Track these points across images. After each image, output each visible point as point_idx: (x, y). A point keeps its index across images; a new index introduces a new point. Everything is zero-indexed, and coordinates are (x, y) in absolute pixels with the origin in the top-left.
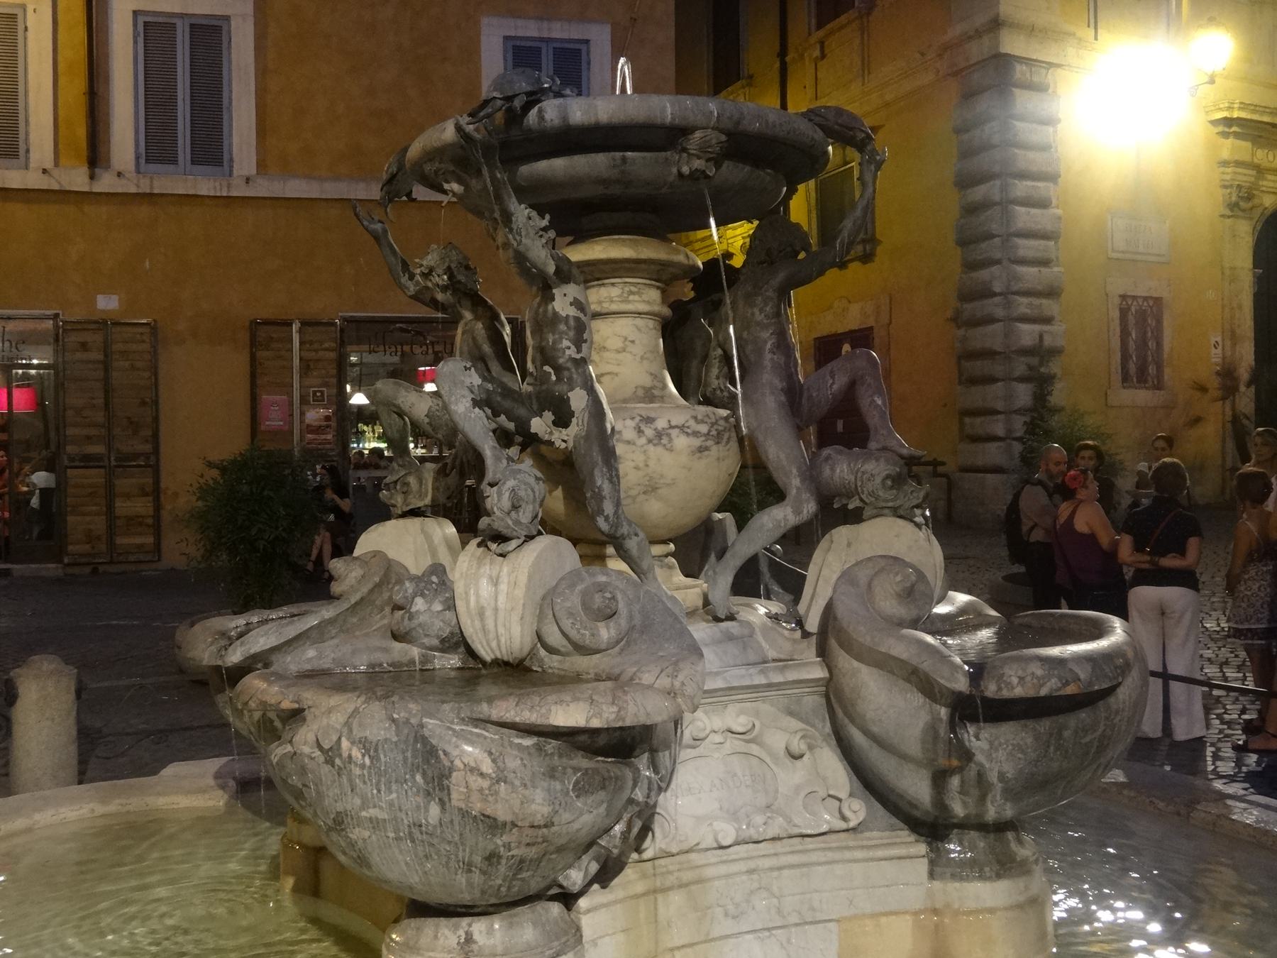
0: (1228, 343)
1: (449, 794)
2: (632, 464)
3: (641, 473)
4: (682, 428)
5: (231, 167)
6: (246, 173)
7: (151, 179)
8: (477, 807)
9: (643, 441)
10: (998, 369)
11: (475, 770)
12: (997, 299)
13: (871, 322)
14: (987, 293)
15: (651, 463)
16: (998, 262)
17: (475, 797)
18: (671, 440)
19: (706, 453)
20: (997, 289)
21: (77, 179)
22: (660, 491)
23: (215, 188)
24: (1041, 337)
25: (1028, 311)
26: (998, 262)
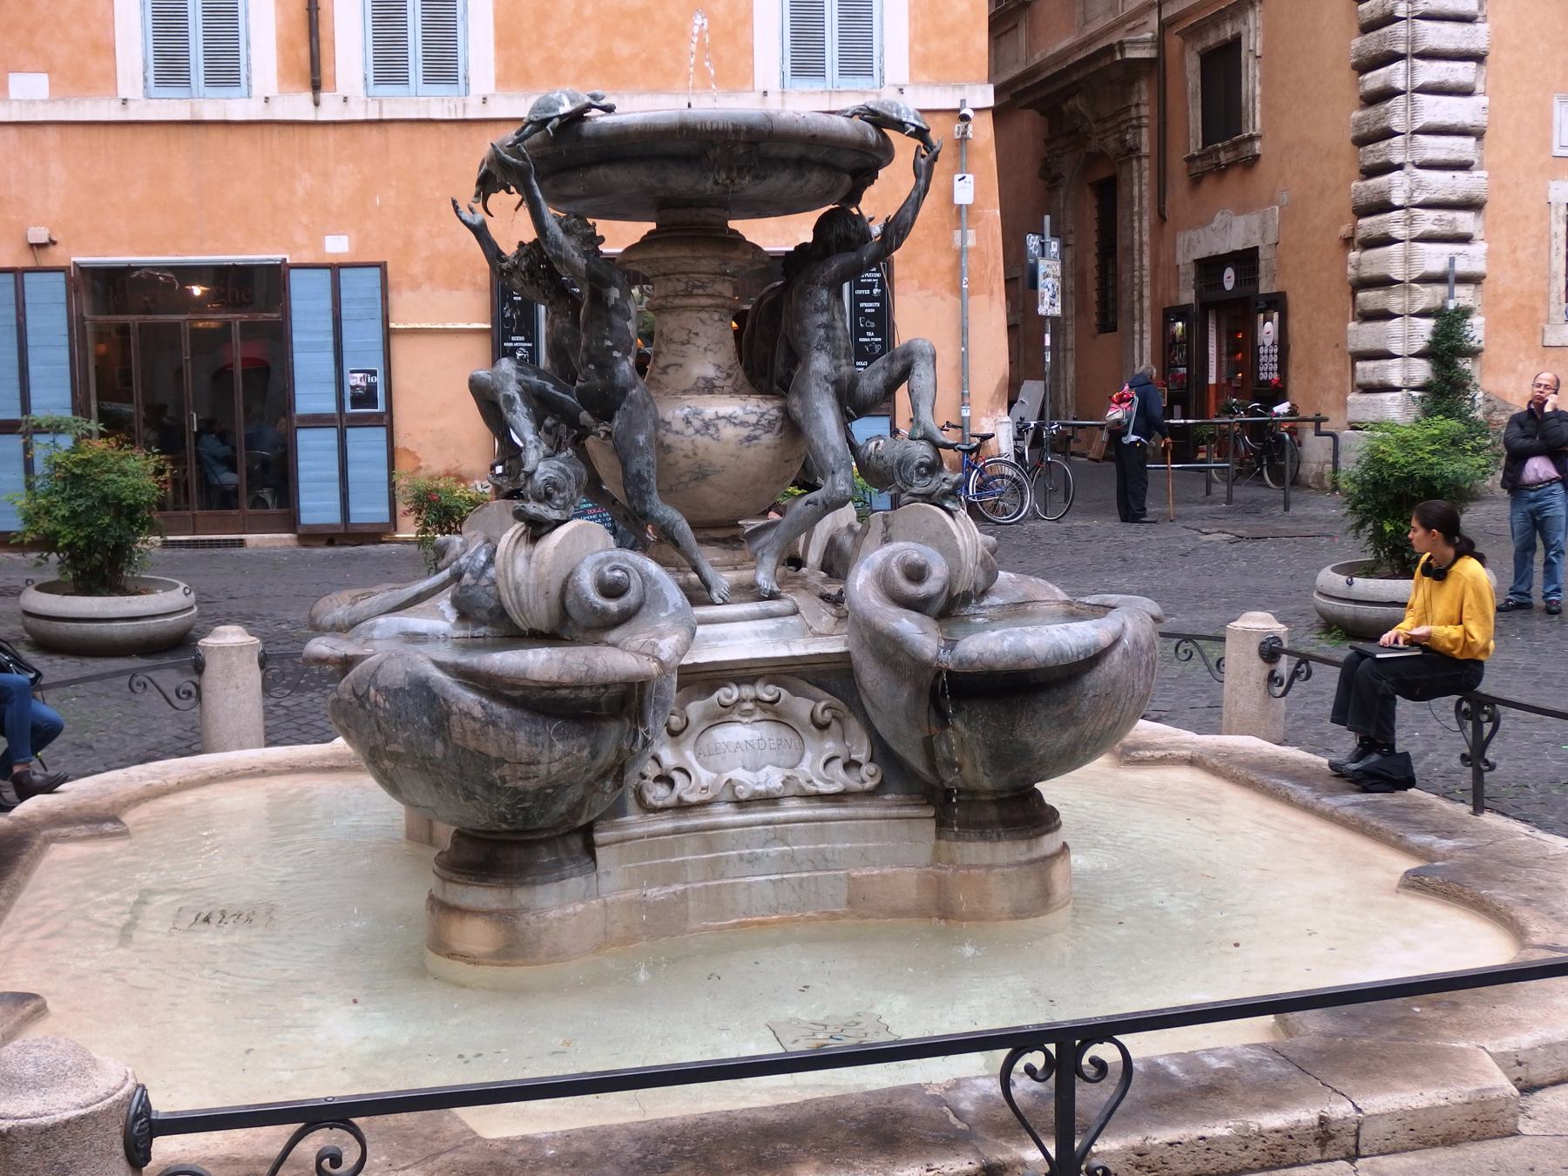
1: (450, 734)
2: (682, 453)
3: (691, 461)
4: (729, 419)
5: (467, 85)
6: (484, 92)
7: (380, 102)
8: (472, 744)
9: (691, 431)
10: (1395, 302)
11: (468, 714)
12: (1395, 214)
13: (1255, 241)
14: (1384, 206)
15: (700, 452)
16: (1400, 167)
17: (469, 736)
18: (718, 430)
19: (755, 442)
20: (1397, 202)
21: (299, 106)
22: (710, 478)
23: (450, 110)
24: (1452, 261)
25: (1435, 228)
26: (1400, 167)
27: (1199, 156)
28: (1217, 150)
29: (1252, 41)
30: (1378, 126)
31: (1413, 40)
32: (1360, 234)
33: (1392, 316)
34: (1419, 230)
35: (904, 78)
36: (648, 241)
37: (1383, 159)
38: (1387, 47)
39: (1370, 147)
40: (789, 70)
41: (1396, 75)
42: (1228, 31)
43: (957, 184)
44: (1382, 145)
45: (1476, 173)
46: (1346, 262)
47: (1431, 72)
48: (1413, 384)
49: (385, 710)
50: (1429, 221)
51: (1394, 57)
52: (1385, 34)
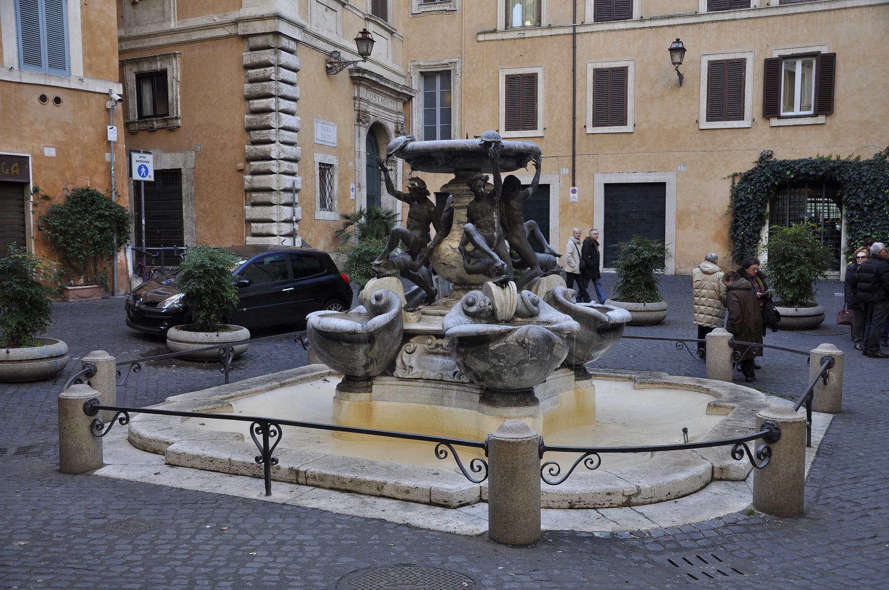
0: (357, 189)
10: (273, 198)
12: (273, 161)
16: (274, 142)
24: (294, 183)
27: (137, 122)
28: (153, 121)
29: (175, 74)
30: (263, 124)
31: (278, 90)
32: (253, 169)
33: (273, 205)
34: (283, 169)
35: (81, 74)
36: (452, 182)
37: (266, 138)
38: (267, 91)
39: (257, 132)
40: (22, 59)
41: (271, 103)
42: (158, 66)
43: (109, 131)
44: (265, 132)
45: (298, 148)
46: (243, 180)
47: (285, 104)
48: (281, 234)
49: (533, 345)
50: (286, 166)
51: (271, 96)
52: (266, 86)
